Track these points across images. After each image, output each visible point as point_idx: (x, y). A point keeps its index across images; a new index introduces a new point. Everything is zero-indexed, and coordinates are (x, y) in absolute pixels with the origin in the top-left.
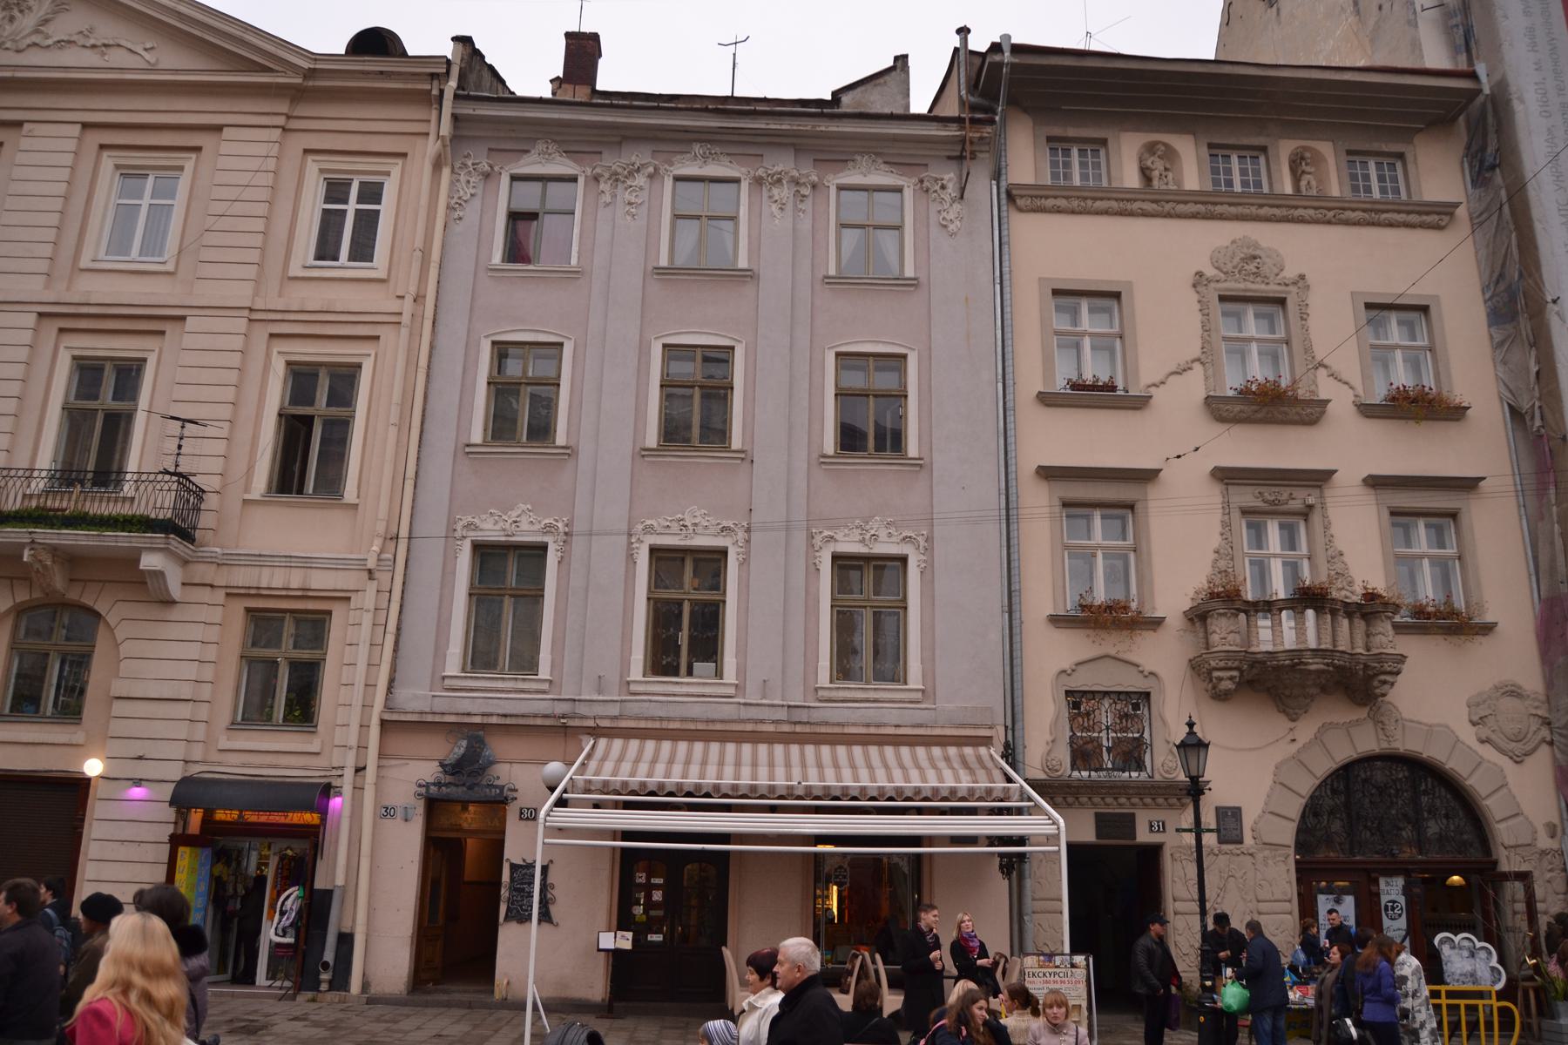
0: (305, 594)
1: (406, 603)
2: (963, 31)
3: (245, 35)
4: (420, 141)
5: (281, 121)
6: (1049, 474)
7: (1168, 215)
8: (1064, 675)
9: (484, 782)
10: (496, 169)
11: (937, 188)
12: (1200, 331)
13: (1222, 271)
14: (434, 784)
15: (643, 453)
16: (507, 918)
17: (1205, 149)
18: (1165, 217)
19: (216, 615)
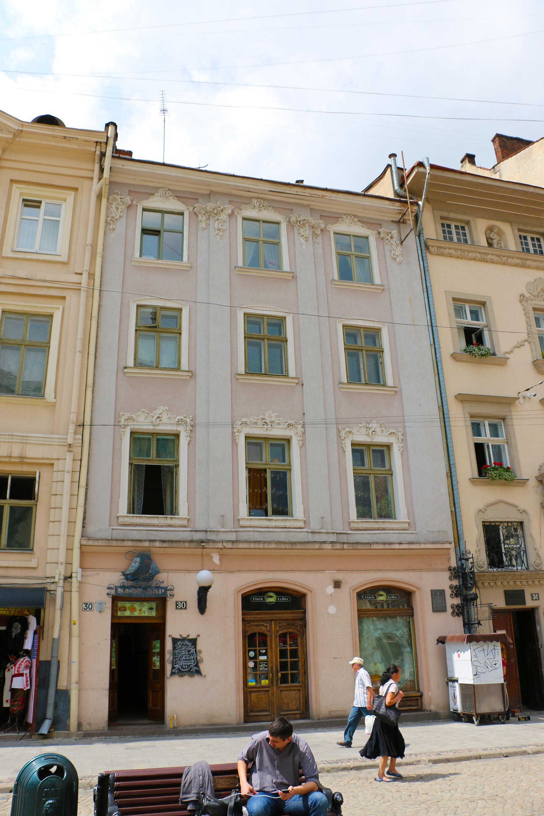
0: (22, 461)
1: (90, 467)
2: (393, 156)
4: (87, 182)
7: (504, 264)
8: (481, 513)
9: (154, 585)
10: (134, 202)
11: (389, 237)
12: (526, 325)
13: (532, 295)
14: (121, 587)
15: (238, 377)
16: (172, 674)
17: (517, 231)
18: (502, 264)
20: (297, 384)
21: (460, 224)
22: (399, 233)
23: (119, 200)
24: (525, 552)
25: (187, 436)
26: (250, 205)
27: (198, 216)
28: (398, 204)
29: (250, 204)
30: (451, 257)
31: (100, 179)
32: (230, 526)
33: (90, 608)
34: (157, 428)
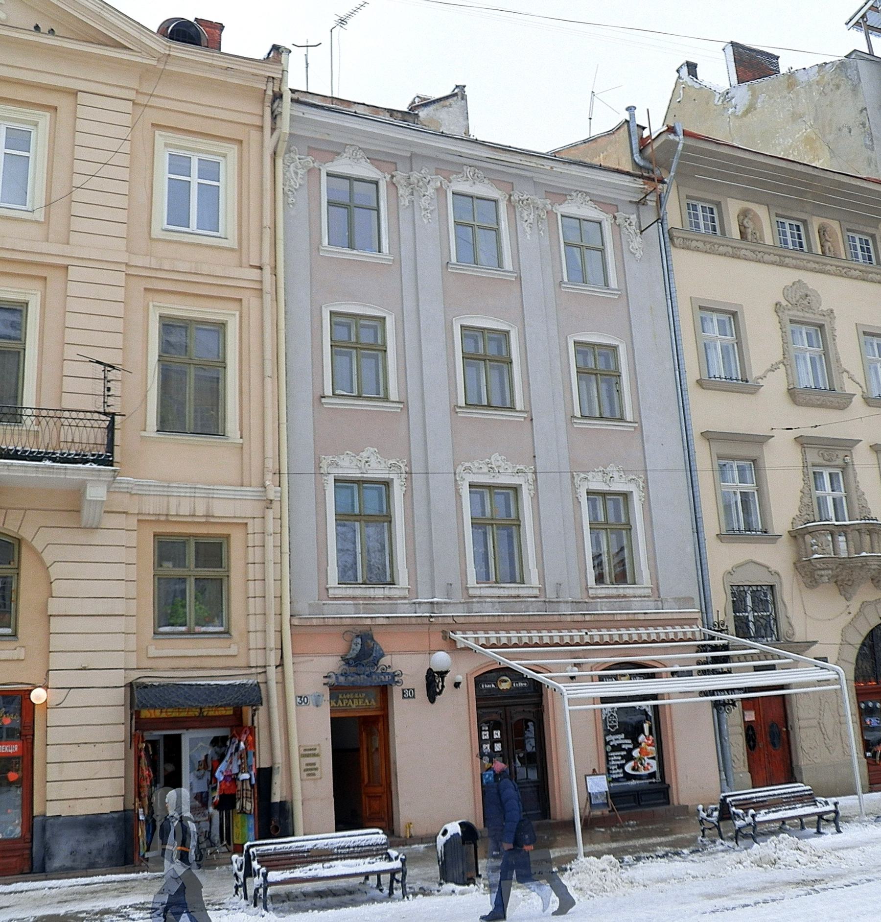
3: (102, 12)
5: (132, 95)
6: (708, 436)
11: (626, 224)
14: (342, 675)
15: (458, 410)
19: (132, 539)
20: (525, 418)
21: (707, 205)
22: (638, 217)
23: (298, 161)
24: (775, 620)
25: (402, 485)
26: (461, 175)
27: (397, 187)
28: (640, 181)
29: (460, 173)
30: (698, 251)
31: (273, 130)
32: (458, 597)
33: (306, 701)
34: (365, 475)
